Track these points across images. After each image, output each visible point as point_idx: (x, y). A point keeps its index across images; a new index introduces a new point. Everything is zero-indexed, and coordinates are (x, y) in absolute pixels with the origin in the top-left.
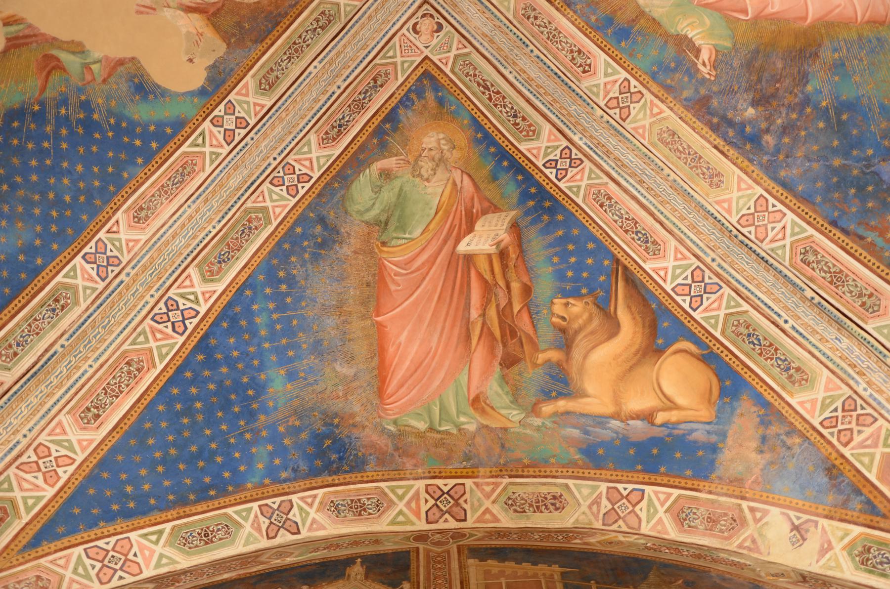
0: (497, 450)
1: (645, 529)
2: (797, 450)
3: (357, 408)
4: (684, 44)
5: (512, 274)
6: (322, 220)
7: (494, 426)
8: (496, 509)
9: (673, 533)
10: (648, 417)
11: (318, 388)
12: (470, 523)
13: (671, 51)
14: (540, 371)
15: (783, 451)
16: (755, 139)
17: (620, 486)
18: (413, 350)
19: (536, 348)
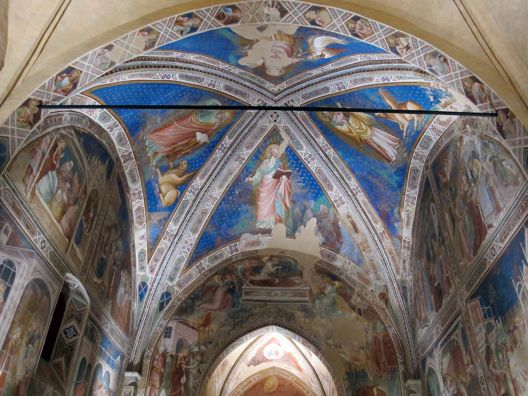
0: (144, 163)
1: (133, 203)
2: (160, 229)
3: (148, 128)
4: (254, 174)
5: (192, 148)
6: (202, 96)
7: (151, 160)
8: (129, 168)
9: (134, 209)
10: (160, 192)
11: (152, 116)
12: (123, 164)
13: (253, 170)
14: (167, 164)
15: (159, 226)
16: (231, 195)
17: (142, 193)
18: (167, 134)
19: (172, 161)
